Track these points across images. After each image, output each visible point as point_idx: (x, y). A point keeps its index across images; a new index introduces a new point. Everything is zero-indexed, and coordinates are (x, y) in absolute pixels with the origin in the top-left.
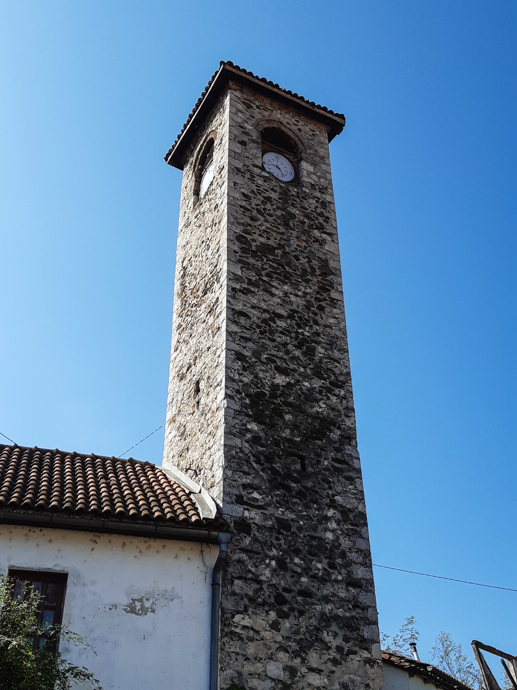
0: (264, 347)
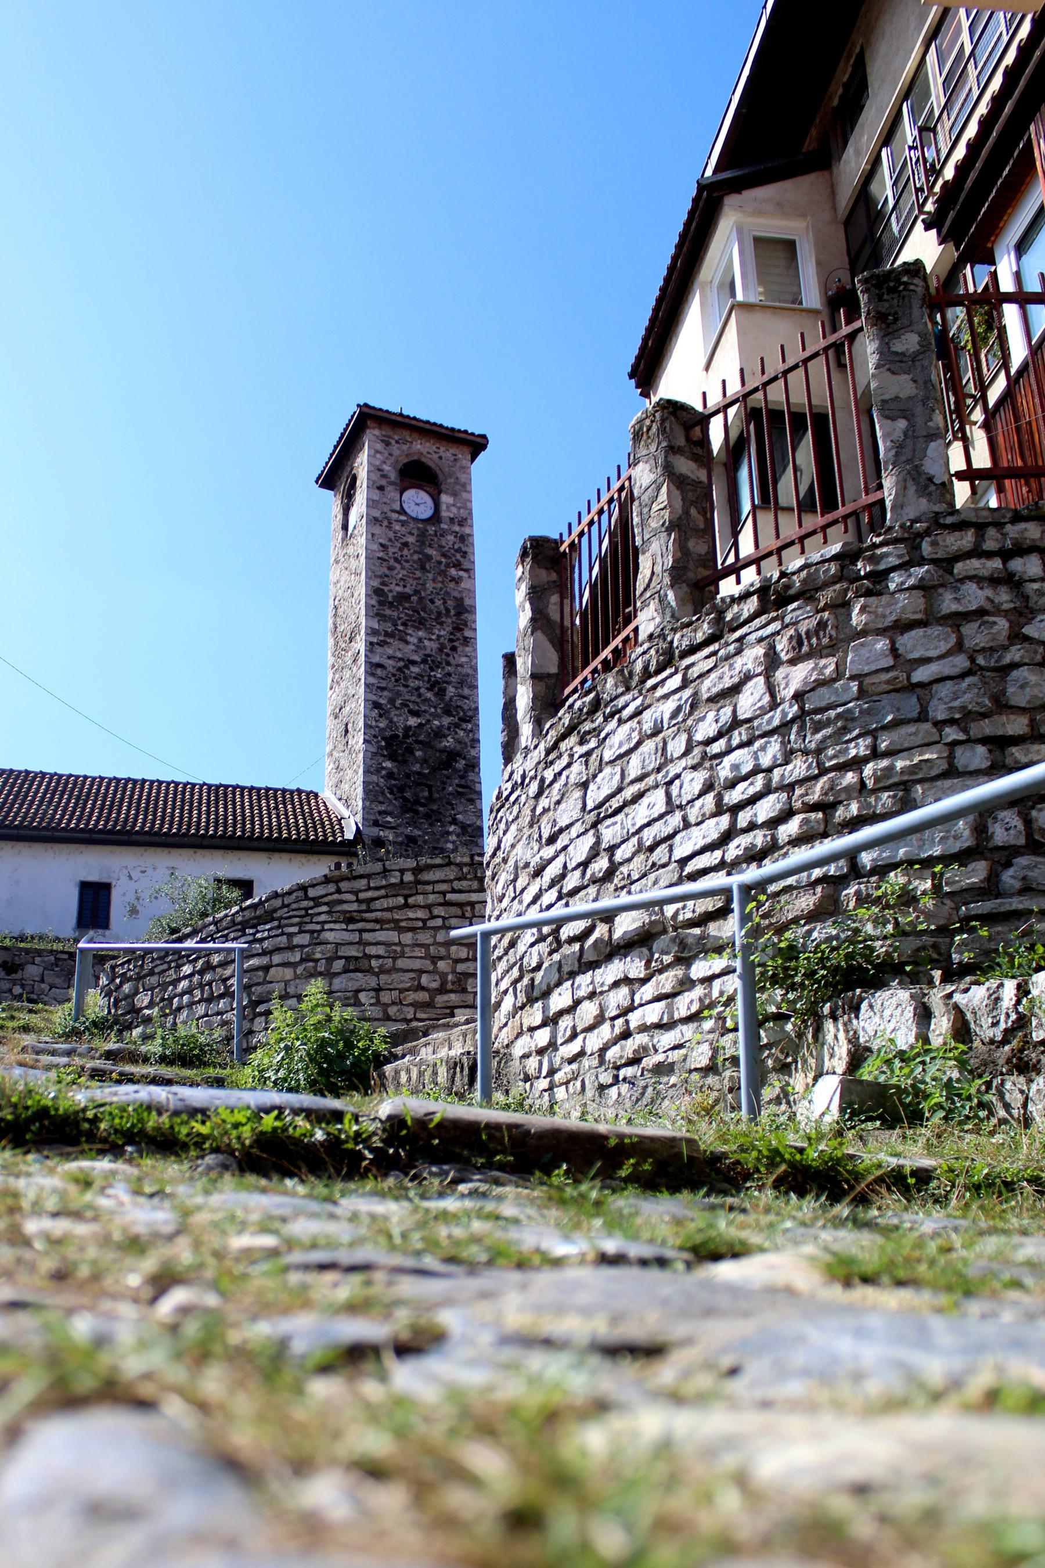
0: (399, 694)
